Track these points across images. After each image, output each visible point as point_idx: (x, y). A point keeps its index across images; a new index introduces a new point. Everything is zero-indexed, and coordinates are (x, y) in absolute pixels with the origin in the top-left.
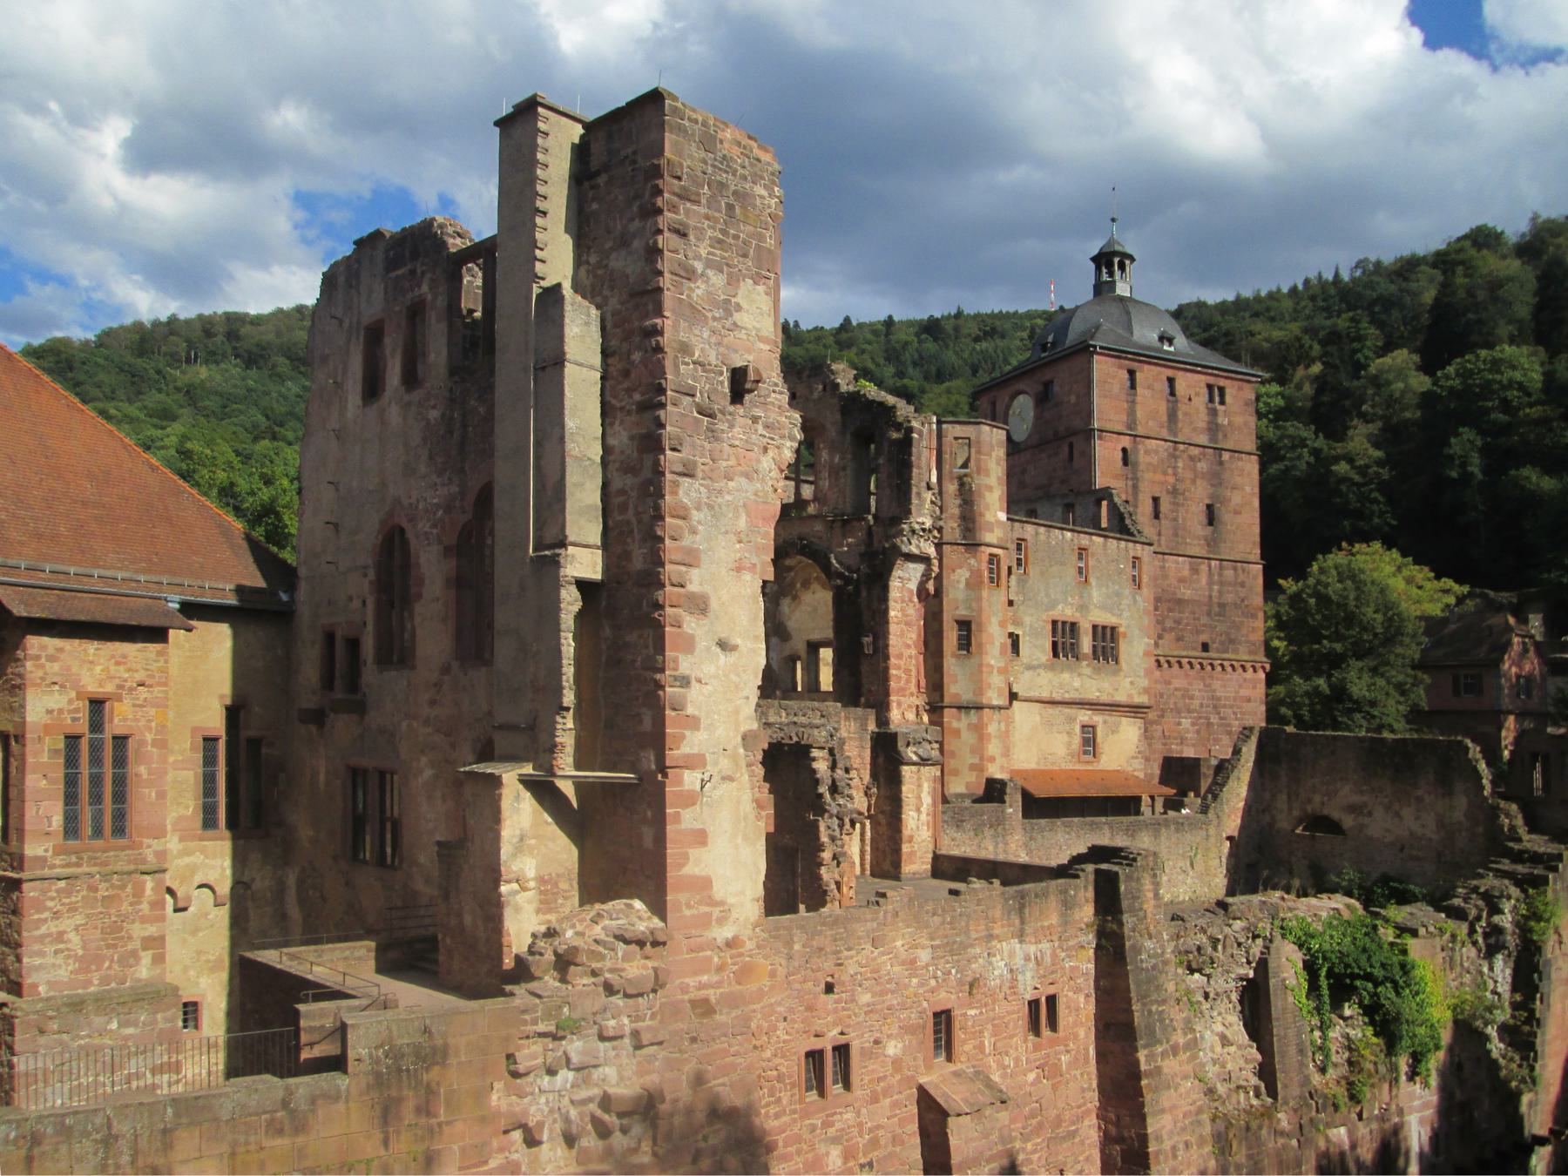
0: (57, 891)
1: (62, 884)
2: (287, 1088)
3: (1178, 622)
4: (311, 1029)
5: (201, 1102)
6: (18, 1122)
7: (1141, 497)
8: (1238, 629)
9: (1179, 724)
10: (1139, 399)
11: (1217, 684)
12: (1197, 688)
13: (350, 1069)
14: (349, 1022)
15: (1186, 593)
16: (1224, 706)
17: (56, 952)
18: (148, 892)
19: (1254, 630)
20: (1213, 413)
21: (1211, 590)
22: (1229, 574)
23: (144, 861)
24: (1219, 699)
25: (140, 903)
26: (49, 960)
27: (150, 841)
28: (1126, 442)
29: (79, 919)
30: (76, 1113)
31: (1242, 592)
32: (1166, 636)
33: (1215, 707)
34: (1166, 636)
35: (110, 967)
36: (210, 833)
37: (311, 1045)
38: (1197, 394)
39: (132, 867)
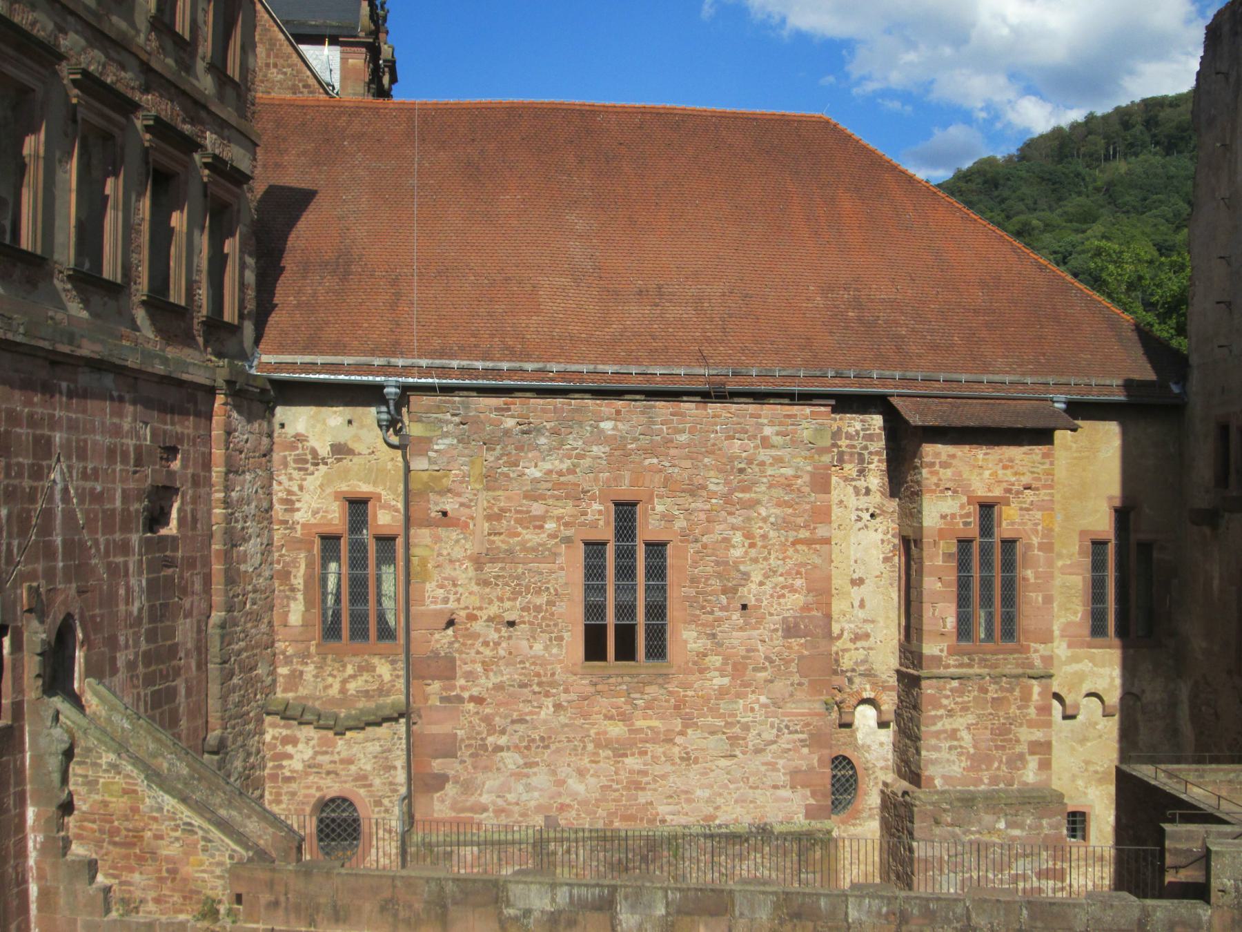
0: (951, 690)
1: (955, 683)
2: (1145, 911)
4: (1177, 852)
5: (1055, 909)
6: (889, 899)
13: (1213, 900)
14: (1213, 848)
17: (950, 748)
18: (1035, 696)
23: (1031, 666)
25: (1027, 707)
26: (944, 755)
27: (1037, 646)
29: (970, 719)
30: (938, 899)
35: (998, 768)
36: (1099, 640)
37: (1177, 868)
39: (1020, 671)
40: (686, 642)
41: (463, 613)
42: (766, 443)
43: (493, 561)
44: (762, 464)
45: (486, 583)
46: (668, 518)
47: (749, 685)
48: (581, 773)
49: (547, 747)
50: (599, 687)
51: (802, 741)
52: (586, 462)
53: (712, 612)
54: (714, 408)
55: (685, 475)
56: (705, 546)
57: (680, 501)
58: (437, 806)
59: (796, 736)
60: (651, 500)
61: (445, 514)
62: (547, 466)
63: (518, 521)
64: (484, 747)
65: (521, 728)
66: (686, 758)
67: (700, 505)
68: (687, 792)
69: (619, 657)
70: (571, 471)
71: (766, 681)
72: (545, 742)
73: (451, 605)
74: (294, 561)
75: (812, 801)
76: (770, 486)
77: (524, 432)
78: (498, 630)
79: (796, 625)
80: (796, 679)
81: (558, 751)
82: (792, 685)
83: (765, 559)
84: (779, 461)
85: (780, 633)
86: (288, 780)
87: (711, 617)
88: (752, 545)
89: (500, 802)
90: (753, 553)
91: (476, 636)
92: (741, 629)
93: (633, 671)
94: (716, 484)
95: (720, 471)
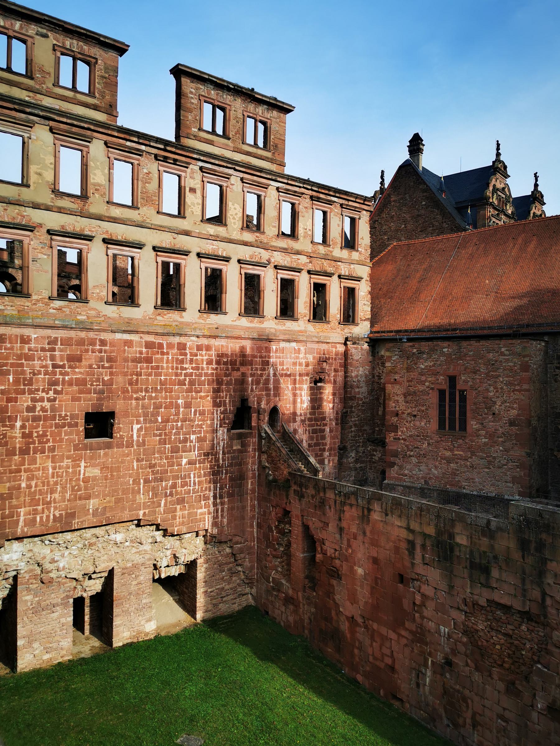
40: (472, 425)
41: (400, 412)
42: (502, 354)
43: (409, 395)
44: (501, 362)
45: (407, 402)
46: (466, 382)
47: (496, 443)
48: (436, 467)
49: (425, 457)
50: (442, 439)
51: (516, 465)
52: (439, 363)
53: (482, 415)
54: (483, 342)
55: (472, 366)
56: (479, 392)
57: (470, 375)
58: (392, 472)
59: (514, 464)
60: (460, 375)
61: (396, 380)
62: (426, 364)
63: (417, 382)
64: (406, 455)
65: (417, 450)
66: (472, 466)
67: (477, 377)
68: (472, 479)
69: (450, 429)
70: (433, 366)
71: (502, 441)
72: (425, 456)
73: (397, 409)
74: (381, 395)
75: (521, 489)
76: (504, 370)
77: (419, 353)
78: (411, 418)
79: (514, 421)
80: (514, 442)
81: (428, 459)
82: (513, 444)
83: (502, 397)
84: (507, 361)
85: (508, 424)
86: (374, 463)
87: (481, 417)
88: (497, 391)
89: (410, 473)
90: (497, 394)
91: (404, 419)
92: (493, 422)
93: (454, 434)
94: (483, 369)
95: (484, 364)
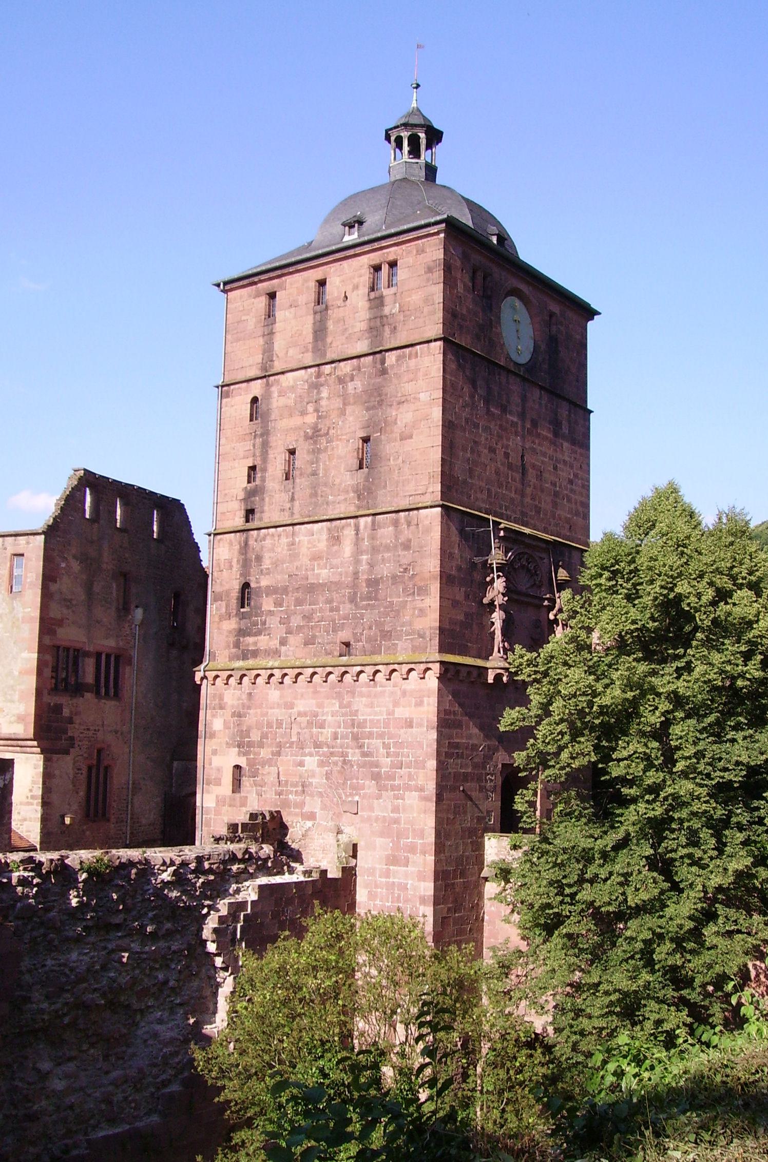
3: (308, 617)
7: (271, 456)
8: (398, 611)
9: (301, 764)
10: (278, 326)
11: (359, 703)
12: (330, 712)
15: (323, 574)
16: (370, 735)
19: (422, 612)
20: (377, 302)
21: (357, 562)
22: (386, 533)
24: (362, 725)
28: (256, 388)
31: (406, 557)
32: (292, 639)
33: (356, 737)
34: (292, 639)
38: (356, 287)
